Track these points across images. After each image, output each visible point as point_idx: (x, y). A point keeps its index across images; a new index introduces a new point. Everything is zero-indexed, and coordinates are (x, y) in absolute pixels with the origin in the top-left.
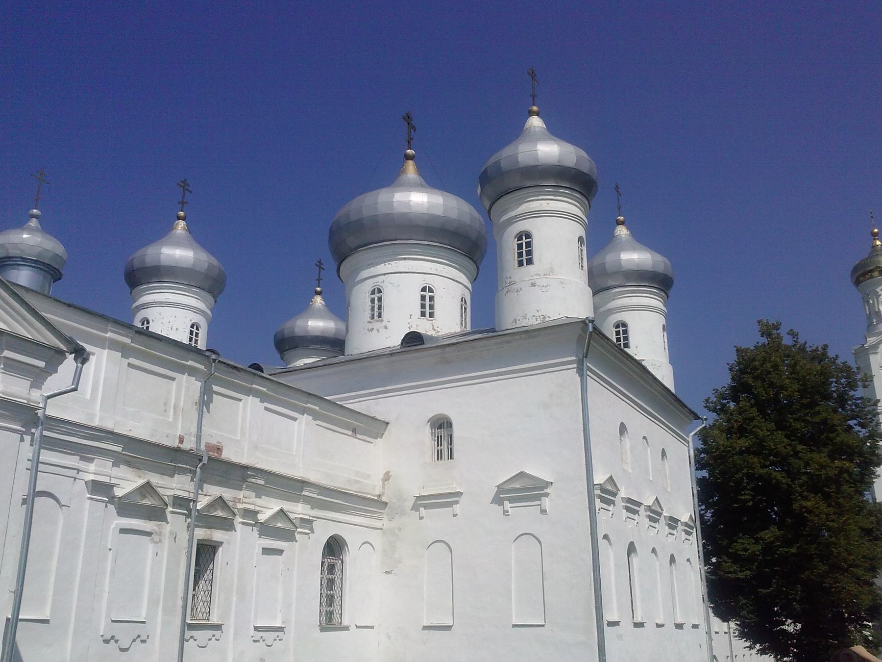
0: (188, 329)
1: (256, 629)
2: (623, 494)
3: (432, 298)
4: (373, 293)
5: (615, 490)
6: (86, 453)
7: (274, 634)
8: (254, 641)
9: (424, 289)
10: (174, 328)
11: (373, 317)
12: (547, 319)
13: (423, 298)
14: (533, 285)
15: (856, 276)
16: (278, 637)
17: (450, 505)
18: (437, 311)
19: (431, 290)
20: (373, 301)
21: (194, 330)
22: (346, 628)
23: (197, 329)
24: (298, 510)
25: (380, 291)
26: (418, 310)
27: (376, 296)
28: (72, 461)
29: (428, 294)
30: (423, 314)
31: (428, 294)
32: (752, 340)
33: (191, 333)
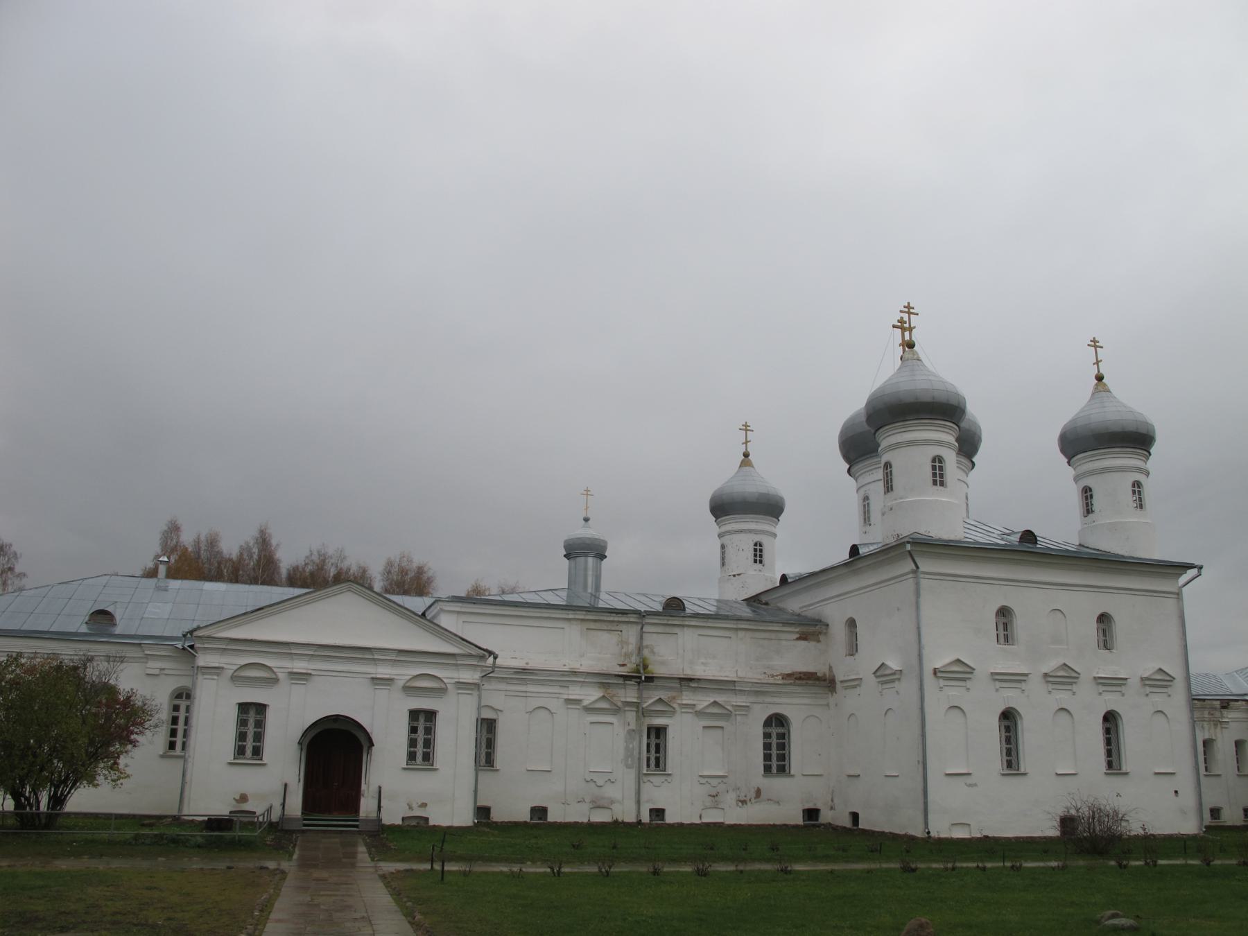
0: (752, 547)
1: (701, 776)
4: (864, 501)
6: (564, 685)
7: (720, 780)
8: (701, 784)
10: (741, 549)
12: (901, 537)
16: (722, 781)
17: (855, 687)
20: (864, 506)
21: (758, 547)
22: (793, 776)
23: (761, 545)
27: (866, 503)
28: (556, 690)
33: (755, 550)
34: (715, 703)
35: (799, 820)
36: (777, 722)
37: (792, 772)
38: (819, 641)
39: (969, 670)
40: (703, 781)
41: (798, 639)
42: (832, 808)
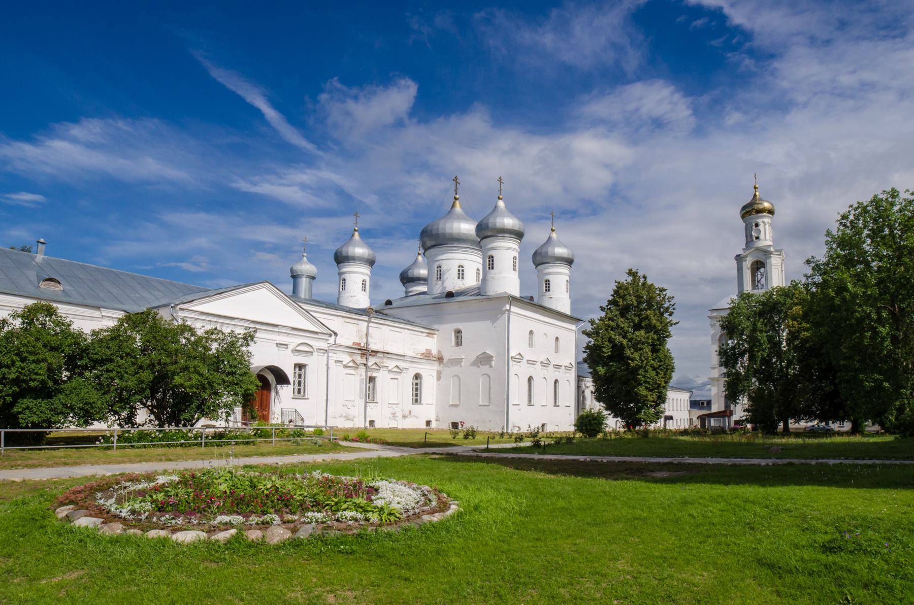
0: (362, 282)
2: (526, 357)
3: (463, 271)
5: (521, 358)
7: (396, 406)
9: (459, 267)
11: (437, 279)
13: (459, 270)
14: (493, 278)
15: (743, 212)
18: (465, 276)
19: (462, 267)
24: (402, 365)
25: (440, 267)
26: (457, 276)
29: (461, 269)
30: (459, 278)
31: (461, 269)
32: (626, 279)
34: (397, 366)
35: (424, 426)
36: (417, 376)
37: (422, 403)
38: (433, 338)
39: (521, 358)
40: (390, 406)
41: (427, 336)
42: (437, 420)
